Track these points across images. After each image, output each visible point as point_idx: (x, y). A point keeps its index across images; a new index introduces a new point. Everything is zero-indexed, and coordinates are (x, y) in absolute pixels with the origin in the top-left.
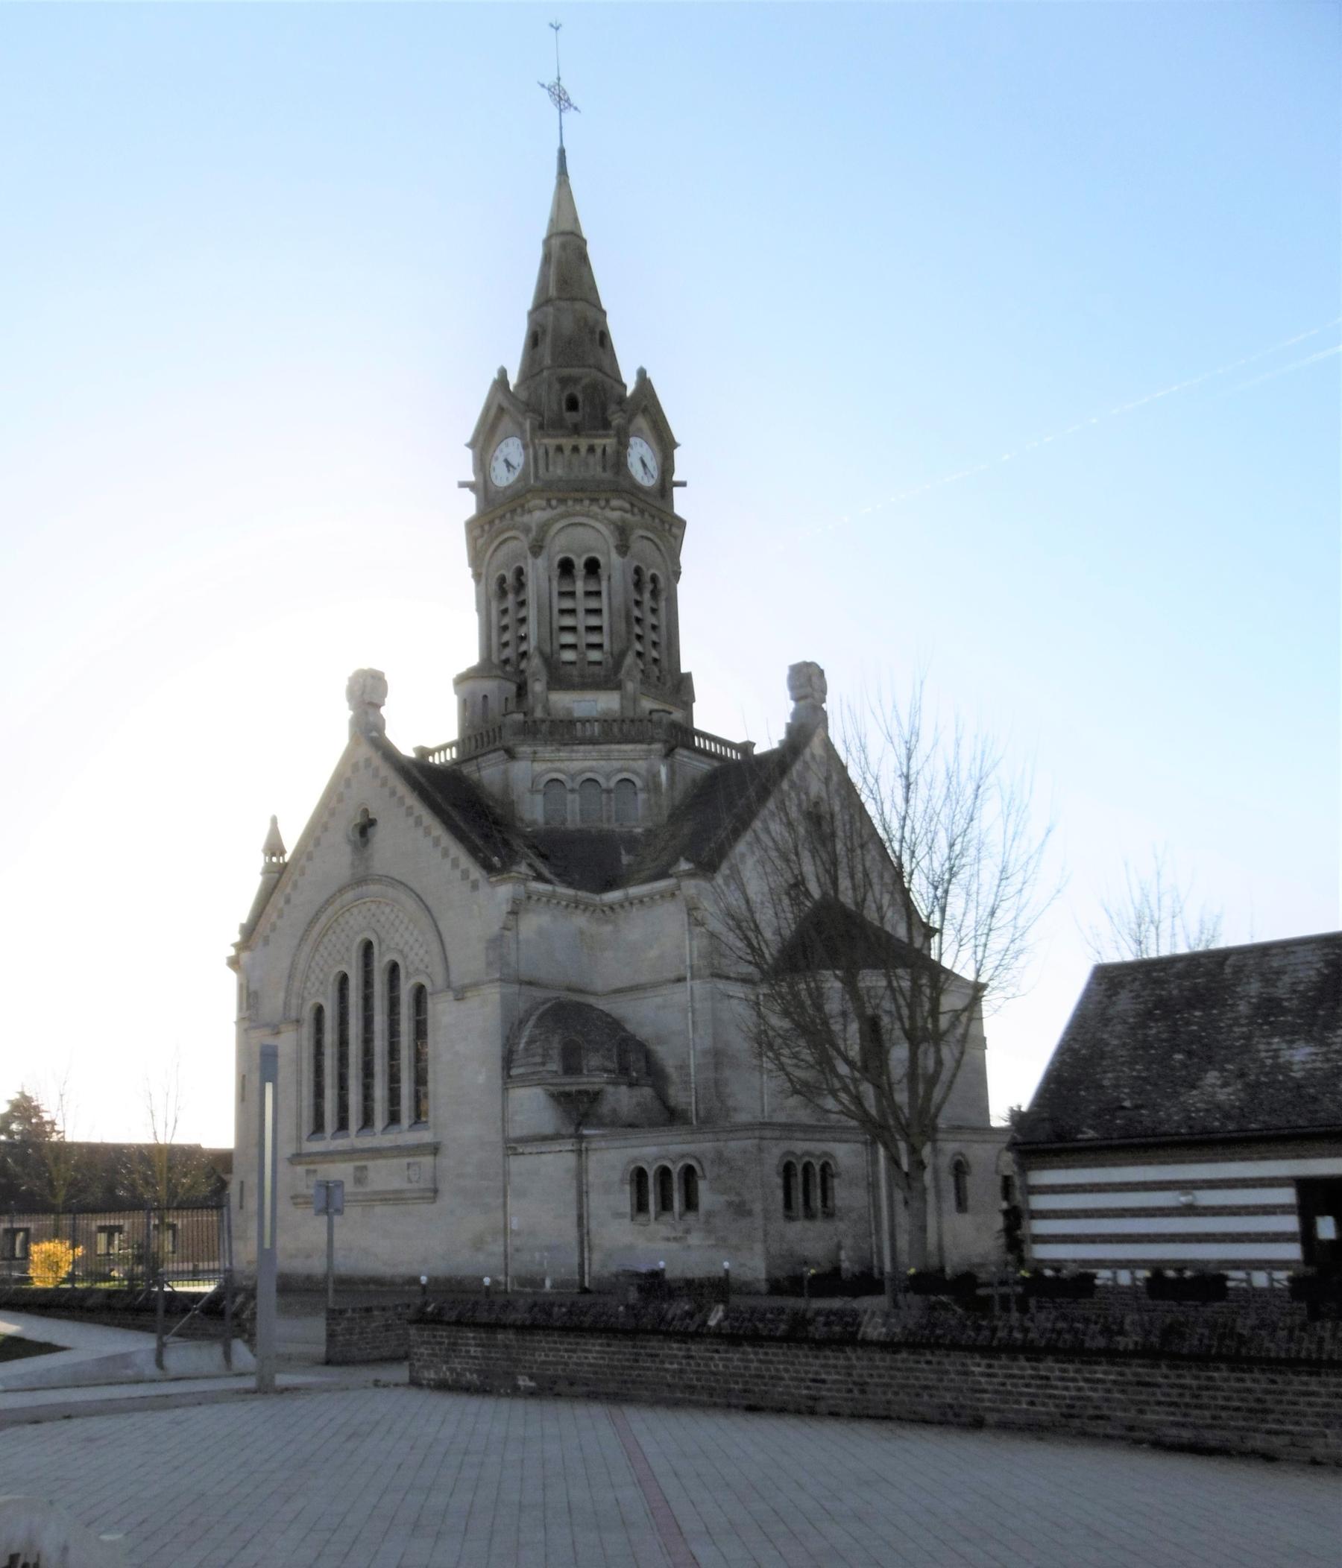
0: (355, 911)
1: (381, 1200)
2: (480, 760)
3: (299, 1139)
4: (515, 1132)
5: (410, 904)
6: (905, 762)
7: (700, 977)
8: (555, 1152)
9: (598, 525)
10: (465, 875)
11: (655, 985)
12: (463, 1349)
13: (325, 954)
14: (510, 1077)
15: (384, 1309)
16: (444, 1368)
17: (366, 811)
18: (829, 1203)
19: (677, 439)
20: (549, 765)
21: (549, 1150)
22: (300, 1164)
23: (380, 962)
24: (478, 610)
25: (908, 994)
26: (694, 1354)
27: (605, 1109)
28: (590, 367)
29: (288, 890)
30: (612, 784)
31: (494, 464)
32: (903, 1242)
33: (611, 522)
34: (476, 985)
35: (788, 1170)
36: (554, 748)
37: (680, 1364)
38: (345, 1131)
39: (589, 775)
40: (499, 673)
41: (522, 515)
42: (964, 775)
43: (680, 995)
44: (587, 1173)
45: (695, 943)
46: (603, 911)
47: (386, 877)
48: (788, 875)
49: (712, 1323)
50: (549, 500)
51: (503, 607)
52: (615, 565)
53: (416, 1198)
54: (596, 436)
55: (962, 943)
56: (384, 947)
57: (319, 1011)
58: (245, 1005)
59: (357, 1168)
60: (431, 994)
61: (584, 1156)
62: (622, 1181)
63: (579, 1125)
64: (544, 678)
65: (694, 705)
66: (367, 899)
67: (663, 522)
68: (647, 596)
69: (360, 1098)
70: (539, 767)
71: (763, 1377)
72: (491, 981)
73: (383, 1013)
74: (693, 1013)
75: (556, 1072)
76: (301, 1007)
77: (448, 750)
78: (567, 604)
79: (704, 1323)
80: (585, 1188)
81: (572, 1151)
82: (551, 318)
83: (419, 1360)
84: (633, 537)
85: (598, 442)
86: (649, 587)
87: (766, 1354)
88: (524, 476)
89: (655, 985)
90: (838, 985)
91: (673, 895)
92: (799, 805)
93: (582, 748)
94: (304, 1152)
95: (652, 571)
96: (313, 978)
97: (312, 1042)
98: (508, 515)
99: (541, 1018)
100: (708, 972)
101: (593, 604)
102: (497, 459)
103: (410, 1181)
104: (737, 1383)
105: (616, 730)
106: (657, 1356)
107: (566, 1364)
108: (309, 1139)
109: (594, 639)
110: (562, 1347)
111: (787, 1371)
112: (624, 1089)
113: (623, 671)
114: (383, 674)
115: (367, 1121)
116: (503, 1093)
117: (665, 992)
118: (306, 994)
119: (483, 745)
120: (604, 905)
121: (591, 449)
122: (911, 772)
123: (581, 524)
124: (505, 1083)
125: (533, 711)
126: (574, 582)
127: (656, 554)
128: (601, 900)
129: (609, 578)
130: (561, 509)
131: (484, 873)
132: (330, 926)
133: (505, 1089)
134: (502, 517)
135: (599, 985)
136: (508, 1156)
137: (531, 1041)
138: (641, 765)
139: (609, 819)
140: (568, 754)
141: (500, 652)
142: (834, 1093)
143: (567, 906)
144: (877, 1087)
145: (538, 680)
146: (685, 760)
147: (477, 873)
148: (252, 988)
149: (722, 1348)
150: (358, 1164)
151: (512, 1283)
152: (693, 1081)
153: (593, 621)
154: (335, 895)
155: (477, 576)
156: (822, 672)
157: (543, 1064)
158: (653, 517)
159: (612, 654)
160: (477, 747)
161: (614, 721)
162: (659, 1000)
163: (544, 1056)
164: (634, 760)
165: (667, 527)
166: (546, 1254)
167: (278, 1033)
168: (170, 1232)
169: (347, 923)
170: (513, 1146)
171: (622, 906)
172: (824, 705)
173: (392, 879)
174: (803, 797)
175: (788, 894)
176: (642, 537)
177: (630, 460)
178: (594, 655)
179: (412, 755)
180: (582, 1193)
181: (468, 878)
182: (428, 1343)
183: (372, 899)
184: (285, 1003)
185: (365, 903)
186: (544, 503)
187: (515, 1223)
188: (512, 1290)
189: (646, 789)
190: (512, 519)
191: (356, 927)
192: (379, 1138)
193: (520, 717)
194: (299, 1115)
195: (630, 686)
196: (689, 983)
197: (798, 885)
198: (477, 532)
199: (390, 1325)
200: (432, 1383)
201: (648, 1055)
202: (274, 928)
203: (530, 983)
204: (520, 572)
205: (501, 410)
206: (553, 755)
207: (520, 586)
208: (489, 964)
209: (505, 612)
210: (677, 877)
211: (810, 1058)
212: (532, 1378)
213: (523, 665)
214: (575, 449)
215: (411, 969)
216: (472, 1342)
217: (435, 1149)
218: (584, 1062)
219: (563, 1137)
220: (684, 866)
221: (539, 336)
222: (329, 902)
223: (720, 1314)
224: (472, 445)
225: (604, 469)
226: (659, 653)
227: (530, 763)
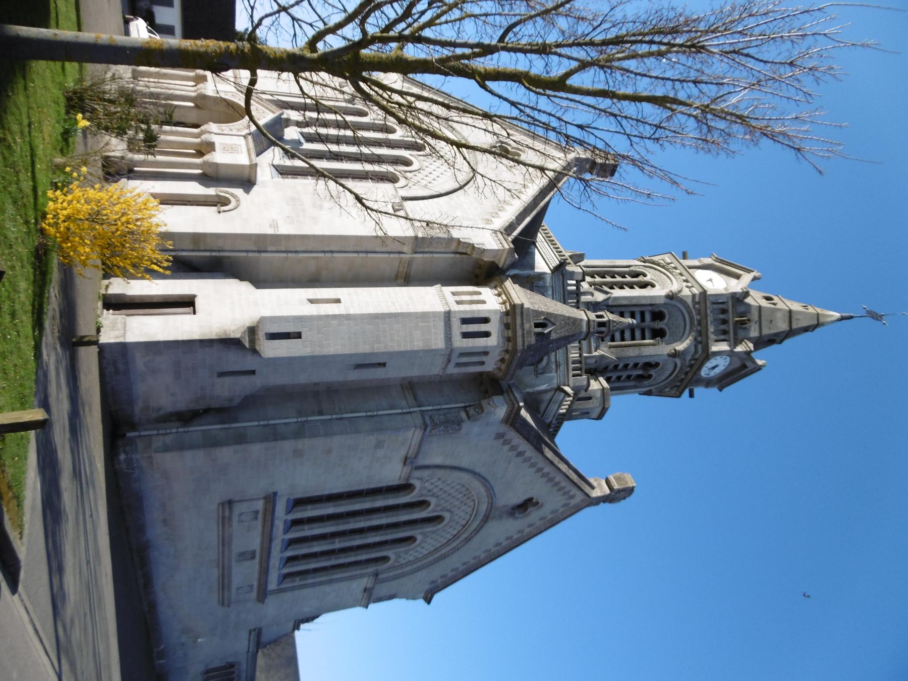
19: (726, 390)
68: (640, 372)
127: (664, 378)
158: (686, 373)
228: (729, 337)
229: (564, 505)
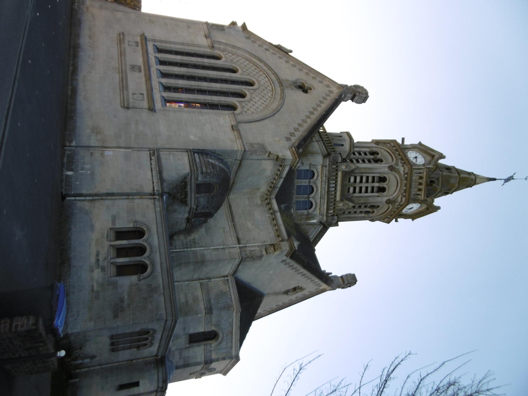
0: (267, 79)
1: (122, 78)
2: (321, 142)
3: (154, 41)
4: (163, 155)
5: (274, 106)
7: (241, 252)
8: (153, 179)
9: (397, 192)
10: (292, 134)
13: (245, 64)
14: (194, 154)
17: (310, 89)
19: (415, 220)
20: (320, 172)
21: (154, 175)
22: (141, 39)
23: (245, 89)
27: (176, 207)
28: (441, 188)
29: (271, 50)
30: (311, 199)
31: (415, 152)
36: (327, 175)
38: (159, 63)
41: (401, 162)
43: (231, 241)
44: (140, 198)
45: (257, 248)
46: (267, 199)
50: (407, 174)
51: (367, 154)
52: (382, 199)
53: (123, 97)
54: (425, 192)
56: (252, 91)
57: (218, 58)
59: (140, 67)
60: (233, 113)
61: (151, 197)
62: (136, 222)
63: (169, 194)
64: (347, 170)
67: (391, 215)
68: (368, 210)
69: (177, 73)
70: (319, 167)
72: (244, 146)
73: (220, 88)
74: (222, 248)
75: (198, 180)
76: (220, 49)
78: (370, 180)
80: (132, 197)
81: (154, 190)
82: (455, 175)
85: (423, 193)
88: (415, 165)
91: (279, 236)
93: (327, 187)
94: (148, 42)
95: (376, 211)
96: (234, 57)
97: (203, 53)
98: (400, 157)
99: (224, 170)
100: (244, 256)
101: (369, 190)
102: (416, 153)
109: (357, 190)
113: (347, 202)
114: (365, 103)
116: (184, 149)
117: (232, 233)
118: (226, 53)
120: (270, 199)
121: (420, 190)
123: (397, 186)
124: (190, 151)
126: (378, 182)
128: (272, 198)
129: (379, 196)
130: (404, 178)
131: (296, 144)
132: (258, 67)
133: (187, 151)
134: (399, 155)
137: (213, 165)
139: (296, 198)
140: (324, 181)
143: (272, 183)
145: (346, 168)
147: (295, 140)
151: (70, 150)
152: (188, 249)
153: (363, 190)
154: (273, 71)
157: (202, 173)
158: (395, 212)
159: (352, 197)
162: (227, 229)
163: (206, 173)
164: (320, 209)
166: (89, 172)
167: (206, 37)
171: (270, 209)
178: (351, 190)
180: (127, 195)
183: (274, 88)
184: (221, 42)
185: (271, 84)
186: (406, 171)
187: (109, 153)
188: (66, 150)
189: (308, 214)
190: (400, 159)
191: (260, 80)
192: (156, 81)
198: (392, 144)
201: (200, 225)
203: (240, 165)
204: (381, 161)
205: (433, 156)
207: (377, 161)
208: (252, 145)
214: (420, 184)
215: (243, 104)
217: (152, 109)
218: (202, 195)
219: (162, 184)
221: (450, 171)
222: (269, 68)
224: (420, 143)
225: (414, 195)
227: (322, 164)
228: (422, 193)
229: (316, 289)
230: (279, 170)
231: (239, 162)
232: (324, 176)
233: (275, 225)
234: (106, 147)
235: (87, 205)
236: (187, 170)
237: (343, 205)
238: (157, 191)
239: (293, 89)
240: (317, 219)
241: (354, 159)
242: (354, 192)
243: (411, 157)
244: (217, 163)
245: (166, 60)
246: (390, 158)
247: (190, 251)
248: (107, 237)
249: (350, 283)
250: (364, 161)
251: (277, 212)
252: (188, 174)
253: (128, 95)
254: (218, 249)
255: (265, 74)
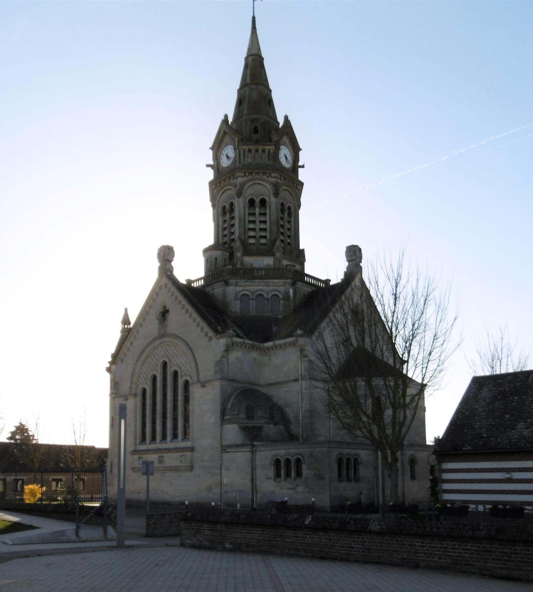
2: (213, 285)
4: (225, 443)
6: (395, 289)
10: (206, 334)
11: (285, 382)
12: (203, 531)
14: (224, 420)
15: (170, 515)
16: (195, 539)
17: (165, 307)
18: (357, 475)
20: (243, 288)
23: (170, 370)
24: (214, 221)
25: (393, 388)
26: (298, 535)
29: (132, 340)
30: (269, 296)
31: (222, 157)
32: (388, 493)
33: (271, 183)
34: (210, 381)
35: (340, 461)
36: (245, 281)
37: (293, 539)
38: (154, 442)
39: (259, 292)
40: (222, 248)
41: (233, 179)
42: (420, 294)
43: (296, 387)
45: (303, 365)
46: (264, 350)
47: (173, 334)
48: (343, 336)
49: (307, 523)
50: (245, 173)
51: (224, 219)
52: (272, 201)
53: (184, 470)
55: (417, 367)
56: (171, 364)
57: (144, 391)
58: (113, 387)
59: (159, 457)
61: (254, 453)
63: (253, 440)
64: (241, 250)
65: (305, 263)
66: (165, 344)
67: (294, 183)
68: (286, 215)
70: (238, 289)
71: (327, 545)
72: (217, 379)
74: (301, 395)
76: (136, 389)
77: (200, 281)
78: (252, 218)
79: (303, 522)
80: (254, 467)
83: (184, 536)
84: (281, 190)
86: (287, 212)
87: (329, 536)
88: (234, 162)
89: (285, 382)
90: (363, 383)
91: (294, 344)
92: (349, 306)
93: (257, 281)
95: (289, 205)
96: (142, 376)
98: (227, 180)
101: (263, 219)
102: (223, 155)
103: (181, 462)
104: (316, 547)
105: (271, 273)
106: (284, 536)
107: (245, 538)
108: (140, 444)
109: (263, 234)
110: (244, 531)
111: (337, 543)
112: (271, 426)
113: (275, 248)
115: (164, 437)
118: (139, 383)
119: (215, 279)
120: (265, 348)
122: (397, 293)
123: (259, 184)
125: (236, 264)
128: (263, 346)
129: (270, 207)
130: (250, 177)
131: (214, 334)
132: (149, 355)
133: (222, 425)
134: (225, 180)
135: (262, 382)
136: (223, 453)
137: (233, 405)
138: (282, 289)
140: (251, 284)
141: (223, 239)
142: (360, 429)
143: (249, 348)
144: (379, 426)
145: (239, 251)
146: (301, 287)
147: (211, 334)
148: (116, 380)
149: (310, 533)
150: (160, 455)
151: (224, 505)
153: (263, 226)
155: (214, 206)
156: (360, 250)
157: (238, 414)
158: (289, 181)
159: (270, 241)
160: (212, 280)
161: (271, 269)
164: (279, 286)
165: (295, 185)
166: (238, 494)
168: (82, 482)
169: (156, 353)
170: (224, 449)
171: (272, 348)
172: (361, 264)
173: (176, 335)
174: (351, 302)
175: (343, 344)
176: (285, 189)
177: (280, 156)
178: (263, 241)
179: (185, 283)
180: (253, 469)
181: (207, 335)
182: (188, 528)
183: (167, 344)
184: (130, 387)
185: (164, 345)
186: (242, 174)
187: (225, 481)
192: (169, 444)
193: (230, 267)
194: (136, 435)
195: (278, 255)
196: (300, 382)
197: (347, 340)
198: (214, 186)
199: (172, 521)
200: (190, 545)
201: (282, 412)
202: (125, 355)
203: (233, 380)
204: (232, 204)
205: (225, 133)
206: (244, 284)
207: (232, 210)
208: (216, 372)
209: (225, 221)
210: (296, 337)
211: (350, 414)
212: (231, 544)
213: (232, 245)
215: (183, 374)
216: (206, 528)
217: (192, 449)
220: (299, 332)
222: (149, 344)
223: (310, 519)
226: (291, 240)
227: (234, 287)
230: (237, 345)
231: (230, 382)
232: (246, 283)
233: (285, 346)
234: (221, 483)
235: (259, 495)
236: (236, 426)
237: (279, 252)
238: (250, 449)
239: (167, 325)
240: (290, 289)
241: (230, 237)
242: (265, 237)
243: (227, 163)
244: (231, 402)
245: (151, 435)
246: (229, 192)
247: (302, 421)
248: (279, 483)
249: (355, 253)
250: (233, 225)
251: (275, 344)
252: (239, 425)
253: (182, 466)
254: (302, 398)
255: (155, 349)
